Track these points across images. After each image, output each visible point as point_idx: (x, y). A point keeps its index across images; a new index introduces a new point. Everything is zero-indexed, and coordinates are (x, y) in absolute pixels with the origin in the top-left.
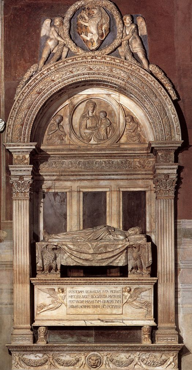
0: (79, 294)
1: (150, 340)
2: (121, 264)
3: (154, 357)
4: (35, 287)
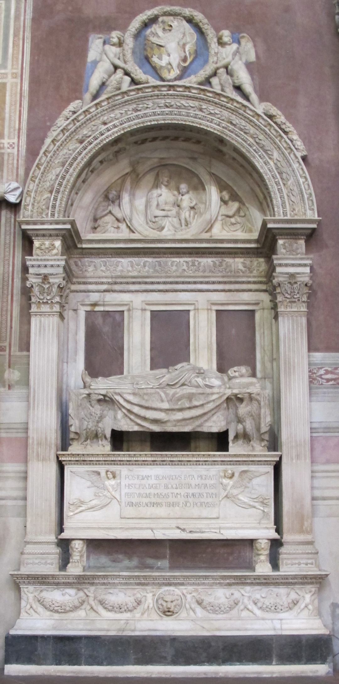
0: (143, 482)
1: (269, 565)
2: (215, 430)
3: (275, 596)
4: (66, 467)
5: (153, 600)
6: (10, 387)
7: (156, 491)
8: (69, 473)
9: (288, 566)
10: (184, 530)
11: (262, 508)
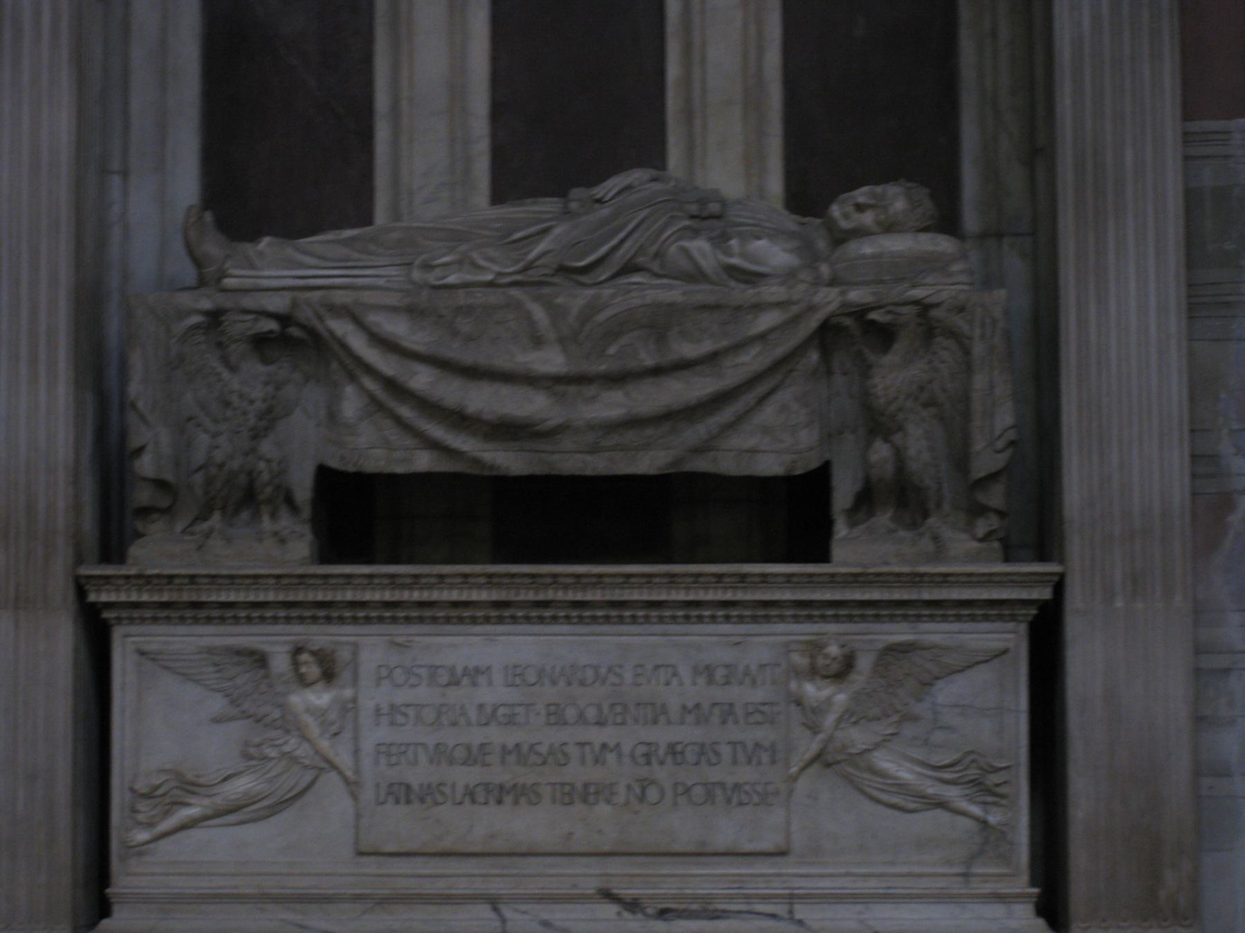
2: (770, 465)
4: (117, 634)
7: (512, 737)
11: (976, 810)
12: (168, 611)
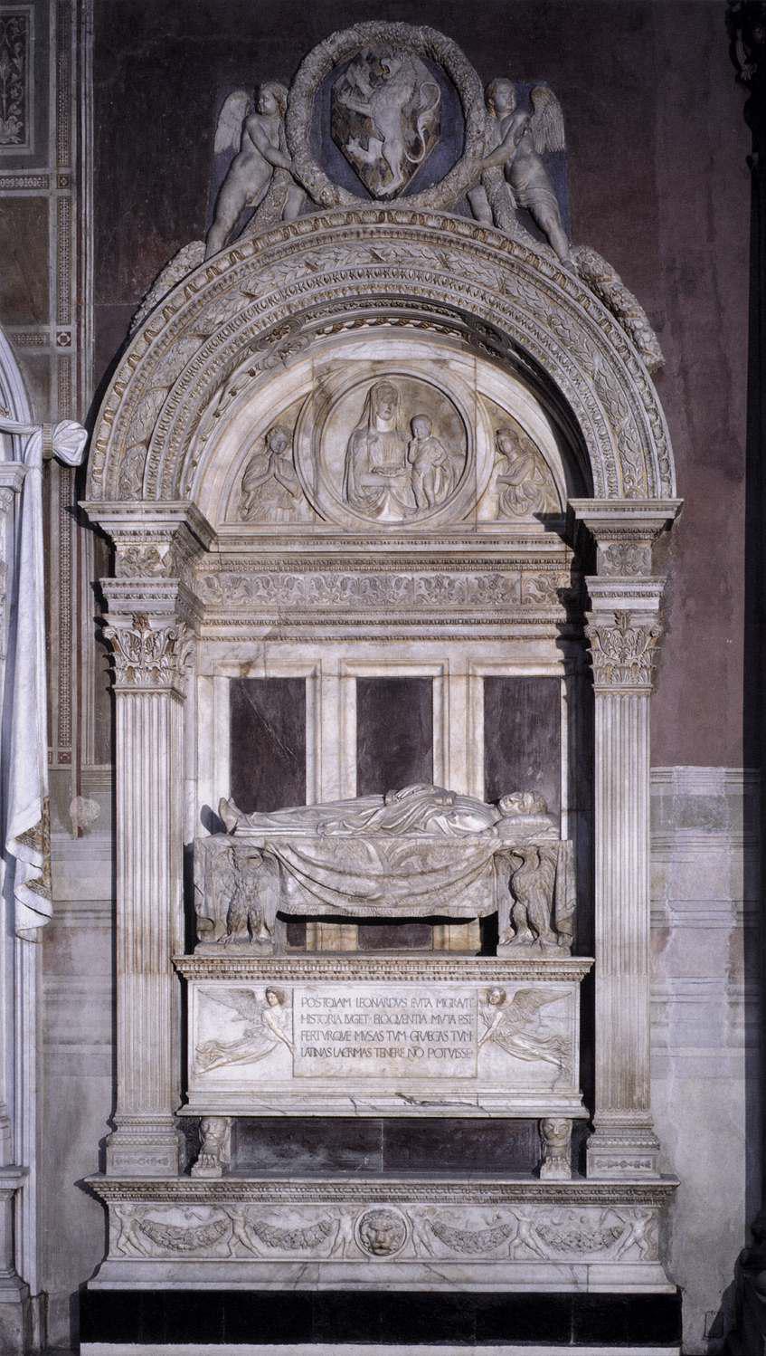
0: (334, 1011)
5: (353, 1227)
6: (81, 833)
7: (359, 1029)
8: (196, 994)
9: (603, 1168)
10: (411, 1100)
12: (211, 974)
